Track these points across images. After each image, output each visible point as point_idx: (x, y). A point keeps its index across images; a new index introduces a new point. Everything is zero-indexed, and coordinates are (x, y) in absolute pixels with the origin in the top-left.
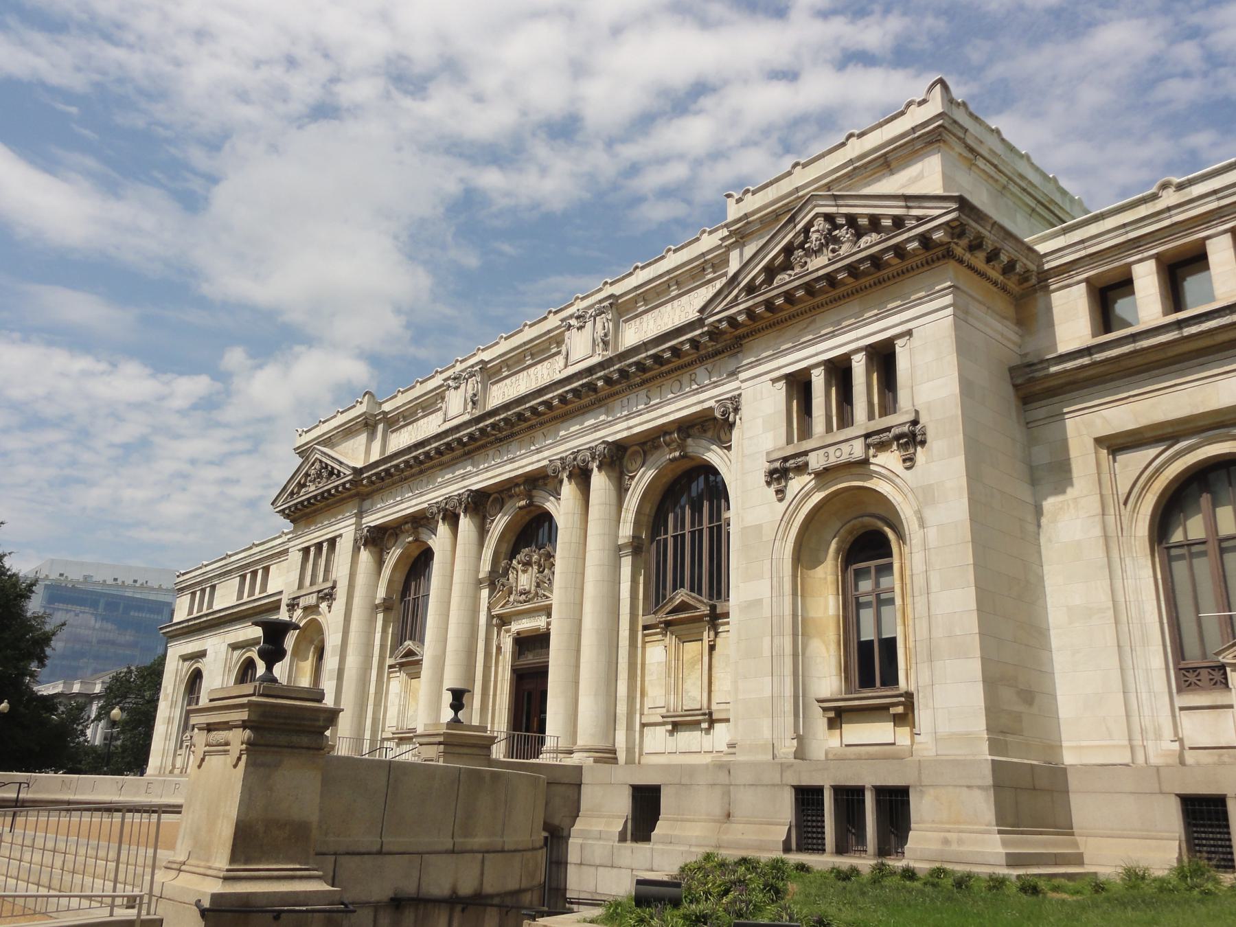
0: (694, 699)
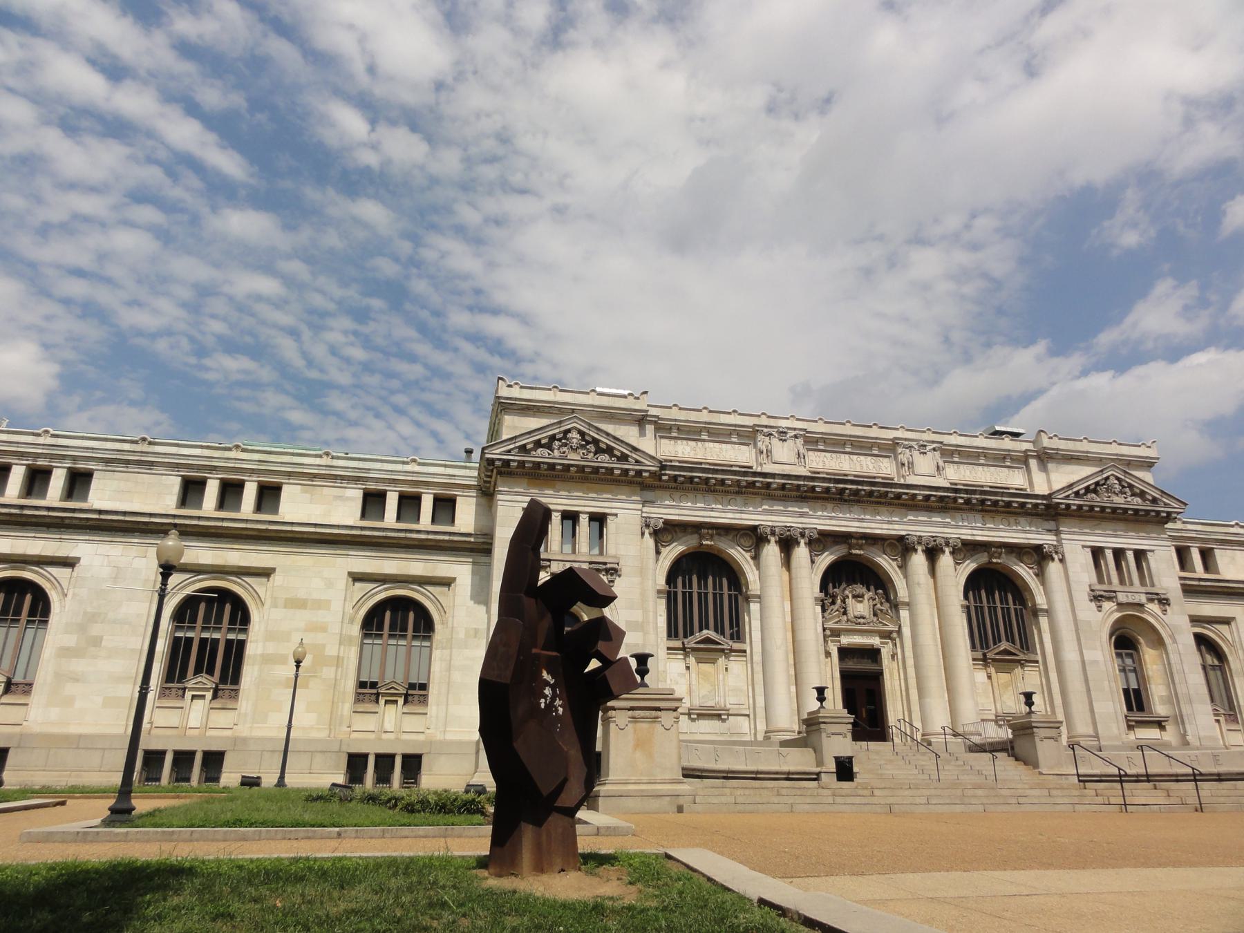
0: (1011, 707)
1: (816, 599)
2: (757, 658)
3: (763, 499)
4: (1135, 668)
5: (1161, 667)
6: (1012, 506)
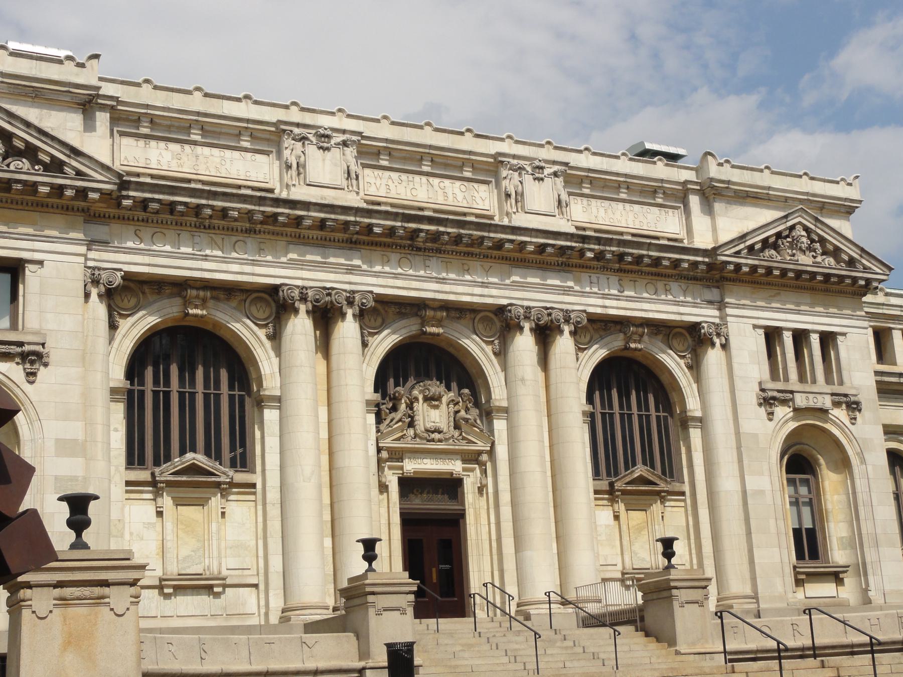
0: (643, 560)
1: (368, 403)
2: (273, 495)
3: (289, 243)
4: (811, 499)
5: (843, 497)
6: (661, 264)
